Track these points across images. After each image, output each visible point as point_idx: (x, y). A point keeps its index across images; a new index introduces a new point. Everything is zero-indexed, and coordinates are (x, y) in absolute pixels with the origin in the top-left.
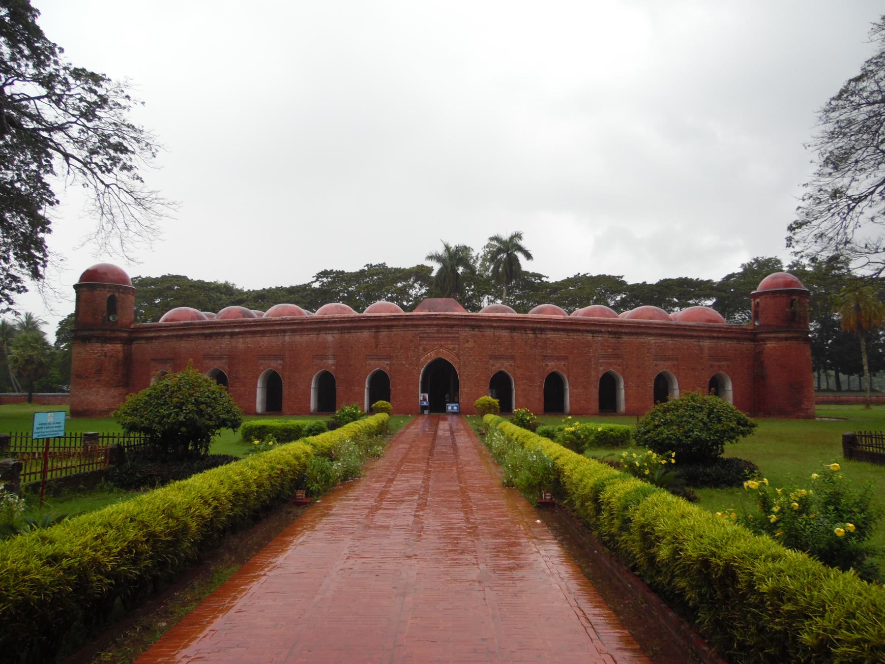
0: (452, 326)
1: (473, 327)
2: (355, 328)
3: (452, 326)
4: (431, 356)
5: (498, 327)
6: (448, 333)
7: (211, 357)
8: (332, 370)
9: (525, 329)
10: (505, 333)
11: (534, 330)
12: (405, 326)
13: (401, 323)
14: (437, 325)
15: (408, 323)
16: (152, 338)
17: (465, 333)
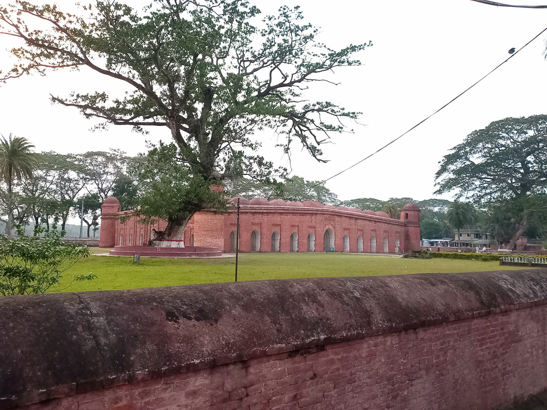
5: (347, 217)
10: (348, 219)
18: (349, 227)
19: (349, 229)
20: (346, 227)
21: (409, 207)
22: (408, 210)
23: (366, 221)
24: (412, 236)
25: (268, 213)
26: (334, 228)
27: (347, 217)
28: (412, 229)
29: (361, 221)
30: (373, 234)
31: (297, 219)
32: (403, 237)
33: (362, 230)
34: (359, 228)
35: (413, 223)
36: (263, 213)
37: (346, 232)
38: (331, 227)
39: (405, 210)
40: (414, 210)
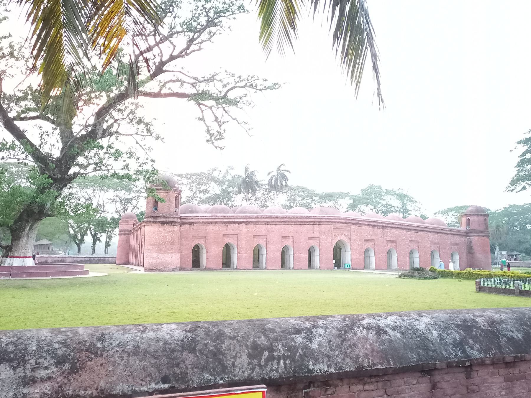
0: (348, 223)
1: (356, 224)
2: (302, 222)
3: (348, 223)
4: (338, 238)
5: (368, 225)
6: (346, 227)
7: (227, 236)
8: (289, 243)
9: (379, 226)
10: (371, 228)
11: (383, 227)
12: (327, 222)
13: (325, 220)
14: (341, 222)
15: (328, 220)
16: (193, 223)
17: (353, 228)
18: (373, 238)
19: (373, 241)
20: (369, 237)
21: (471, 211)
22: (470, 215)
23: (401, 231)
24: (477, 249)
25: (247, 223)
26: (350, 239)
27: (368, 225)
28: (475, 240)
29: (393, 230)
30: (413, 246)
31: (290, 229)
32: (465, 252)
33: (394, 242)
34: (388, 238)
35: (474, 231)
36: (239, 223)
37: (369, 245)
38: (344, 238)
39: (466, 215)
40: (478, 215)
